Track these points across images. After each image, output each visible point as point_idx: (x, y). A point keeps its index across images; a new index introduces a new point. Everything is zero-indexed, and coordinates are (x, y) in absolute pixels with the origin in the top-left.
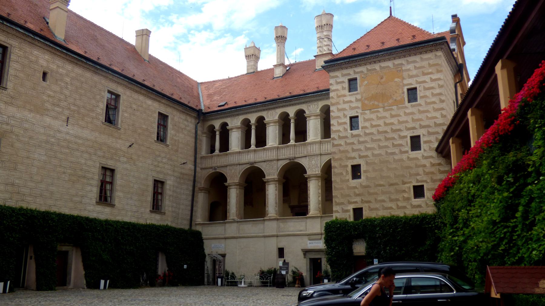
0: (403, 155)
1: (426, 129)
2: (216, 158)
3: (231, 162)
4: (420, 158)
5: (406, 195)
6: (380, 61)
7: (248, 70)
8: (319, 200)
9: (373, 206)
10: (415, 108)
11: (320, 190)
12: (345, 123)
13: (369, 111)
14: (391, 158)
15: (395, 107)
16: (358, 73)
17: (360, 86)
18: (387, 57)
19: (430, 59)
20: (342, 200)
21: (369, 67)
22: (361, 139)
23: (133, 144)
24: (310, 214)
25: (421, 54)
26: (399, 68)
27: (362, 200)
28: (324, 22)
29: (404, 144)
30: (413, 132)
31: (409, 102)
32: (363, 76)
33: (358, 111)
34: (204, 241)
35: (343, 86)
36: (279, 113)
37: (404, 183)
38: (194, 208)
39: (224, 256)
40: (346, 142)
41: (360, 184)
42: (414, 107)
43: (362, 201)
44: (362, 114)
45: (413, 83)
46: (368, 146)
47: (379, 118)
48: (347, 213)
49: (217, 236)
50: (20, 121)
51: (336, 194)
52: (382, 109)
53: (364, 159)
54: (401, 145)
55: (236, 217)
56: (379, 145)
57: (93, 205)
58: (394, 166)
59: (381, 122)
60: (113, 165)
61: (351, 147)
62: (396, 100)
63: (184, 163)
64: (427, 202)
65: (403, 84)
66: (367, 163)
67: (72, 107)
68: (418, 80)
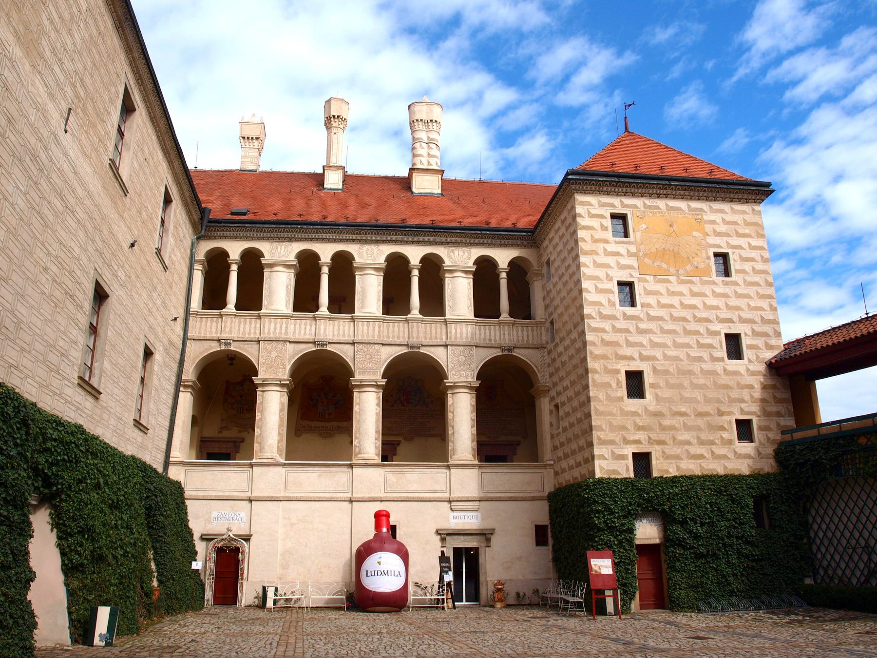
0: (716, 363)
2: (229, 319)
3: (269, 333)
4: (743, 373)
5: (726, 435)
6: (667, 196)
12: (611, 292)
14: (696, 367)
16: (627, 206)
17: (634, 231)
18: (681, 192)
20: (611, 436)
21: (648, 202)
22: (643, 326)
29: (717, 345)
30: (730, 328)
32: (638, 214)
34: (187, 502)
35: (603, 223)
37: (721, 413)
39: (247, 539)
40: (613, 327)
41: (643, 407)
43: (650, 441)
44: (640, 280)
46: (656, 339)
48: (622, 462)
49: (227, 494)
51: (599, 423)
53: (650, 362)
54: (711, 346)
56: (674, 341)
57: (73, 383)
58: (702, 381)
59: (675, 301)
64: (760, 449)
66: (654, 370)
68: (730, 241)
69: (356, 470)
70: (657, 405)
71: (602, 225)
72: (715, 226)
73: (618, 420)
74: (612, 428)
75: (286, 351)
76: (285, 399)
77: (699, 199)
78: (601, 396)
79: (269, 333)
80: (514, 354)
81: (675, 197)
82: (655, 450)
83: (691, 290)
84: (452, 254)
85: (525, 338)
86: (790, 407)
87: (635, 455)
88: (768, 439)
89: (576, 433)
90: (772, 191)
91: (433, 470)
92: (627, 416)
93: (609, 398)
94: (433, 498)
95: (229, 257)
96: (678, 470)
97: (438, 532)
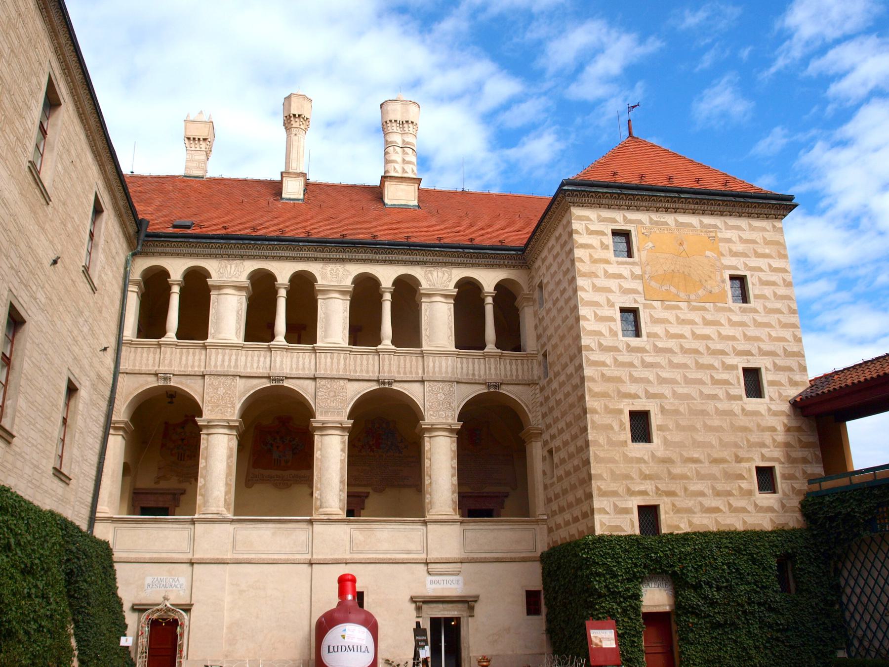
0: (732, 402)
2: (168, 350)
3: (216, 366)
4: (763, 412)
5: (744, 485)
6: (676, 210)
9: (681, 502)
10: (747, 314)
13: (659, 302)
14: (710, 406)
18: (692, 206)
20: (613, 487)
21: (655, 217)
22: (649, 359)
26: (711, 232)
29: (733, 381)
30: (748, 361)
32: (643, 231)
33: (638, 299)
34: (117, 566)
35: (603, 240)
37: (739, 460)
39: (187, 609)
40: (615, 359)
41: (650, 453)
42: (745, 312)
44: (645, 306)
45: (740, 268)
46: (664, 375)
48: (625, 516)
49: (164, 555)
51: (599, 472)
52: (686, 304)
53: (658, 401)
54: (727, 382)
55: (224, 509)
56: (685, 376)
58: (716, 422)
59: (686, 330)
61: (627, 372)
64: (783, 501)
66: (663, 410)
68: (747, 262)
69: (317, 527)
70: (666, 450)
71: (602, 243)
72: (731, 244)
74: (614, 477)
75: (235, 387)
76: (234, 443)
77: (712, 213)
78: (602, 440)
79: (216, 366)
80: (501, 391)
81: (685, 212)
82: (664, 503)
83: (704, 318)
84: (429, 275)
85: (514, 373)
86: (817, 453)
87: (641, 508)
88: (793, 488)
89: (572, 483)
90: (795, 206)
91: (407, 527)
92: (632, 463)
93: (611, 443)
94: (407, 559)
95: (169, 276)
96: (690, 526)
97: (413, 600)
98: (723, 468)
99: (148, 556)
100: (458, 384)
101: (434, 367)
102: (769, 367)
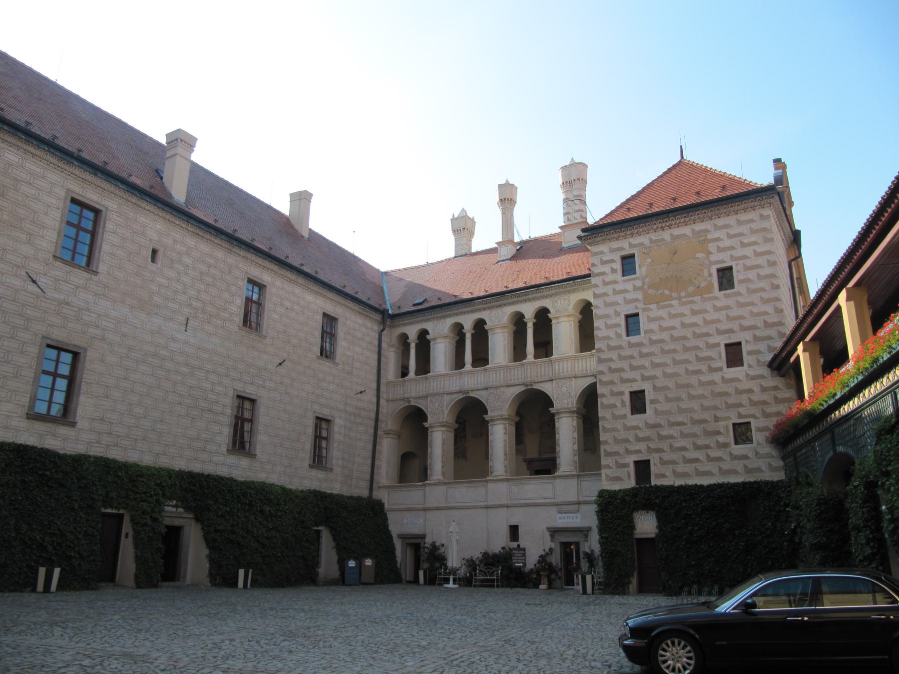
1: (751, 332)
4: (741, 379)
5: (721, 439)
6: (670, 227)
7: (456, 251)
8: (574, 450)
9: (666, 457)
11: (576, 433)
12: (618, 325)
13: (655, 305)
14: (694, 380)
15: (697, 298)
17: (640, 267)
19: (752, 221)
20: (616, 448)
21: (654, 236)
23: (285, 360)
24: (560, 470)
25: (737, 214)
26: (701, 236)
27: (649, 448)
28: (574, 177)
30: (730, 338)
31: (720, 290)
32: (644, 251)
36: (509, 313)
37: (717, 419)
38: (377, 463)
41: (644, 421)
43: (650, 450)
44: (644, 310)
47: (672, 316)
50: (115, 322)
54: (710, 358)
56: (674, 359)
57: (223, 454)
58: (700, 391)
59: (676, 322)
60: (254, 393)
62: (699, 287)
63: (361, 392)
64: (758, 450)
65: (710, 261)
66: (655, 388)
67: (194, 303)
68: (733, 254)
73: (622, 435)
74: (617, 441)
75: (444, 401)
76: (451, 436)
87: (636, 463)
91: (544, 481)
93: (615, 417)
98: (703, 427)
99: (404, 507)
100: (576, 379)
101: (559, 369)
102: (749, 340)
